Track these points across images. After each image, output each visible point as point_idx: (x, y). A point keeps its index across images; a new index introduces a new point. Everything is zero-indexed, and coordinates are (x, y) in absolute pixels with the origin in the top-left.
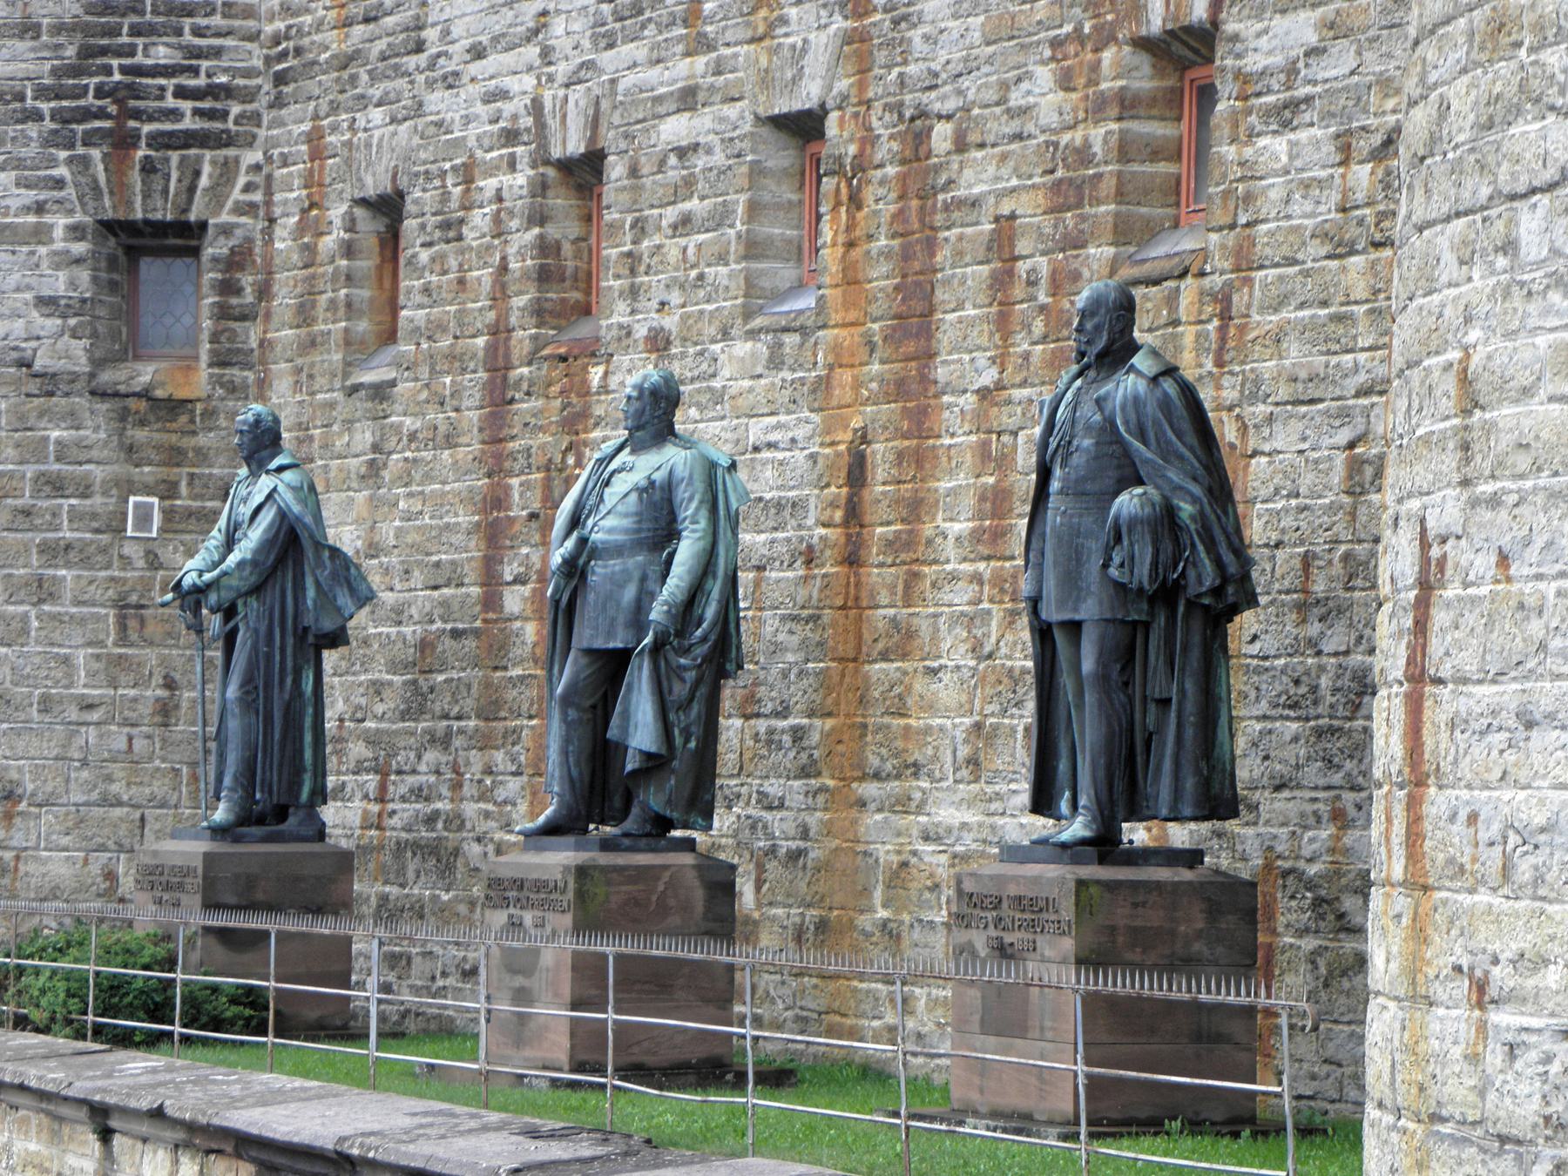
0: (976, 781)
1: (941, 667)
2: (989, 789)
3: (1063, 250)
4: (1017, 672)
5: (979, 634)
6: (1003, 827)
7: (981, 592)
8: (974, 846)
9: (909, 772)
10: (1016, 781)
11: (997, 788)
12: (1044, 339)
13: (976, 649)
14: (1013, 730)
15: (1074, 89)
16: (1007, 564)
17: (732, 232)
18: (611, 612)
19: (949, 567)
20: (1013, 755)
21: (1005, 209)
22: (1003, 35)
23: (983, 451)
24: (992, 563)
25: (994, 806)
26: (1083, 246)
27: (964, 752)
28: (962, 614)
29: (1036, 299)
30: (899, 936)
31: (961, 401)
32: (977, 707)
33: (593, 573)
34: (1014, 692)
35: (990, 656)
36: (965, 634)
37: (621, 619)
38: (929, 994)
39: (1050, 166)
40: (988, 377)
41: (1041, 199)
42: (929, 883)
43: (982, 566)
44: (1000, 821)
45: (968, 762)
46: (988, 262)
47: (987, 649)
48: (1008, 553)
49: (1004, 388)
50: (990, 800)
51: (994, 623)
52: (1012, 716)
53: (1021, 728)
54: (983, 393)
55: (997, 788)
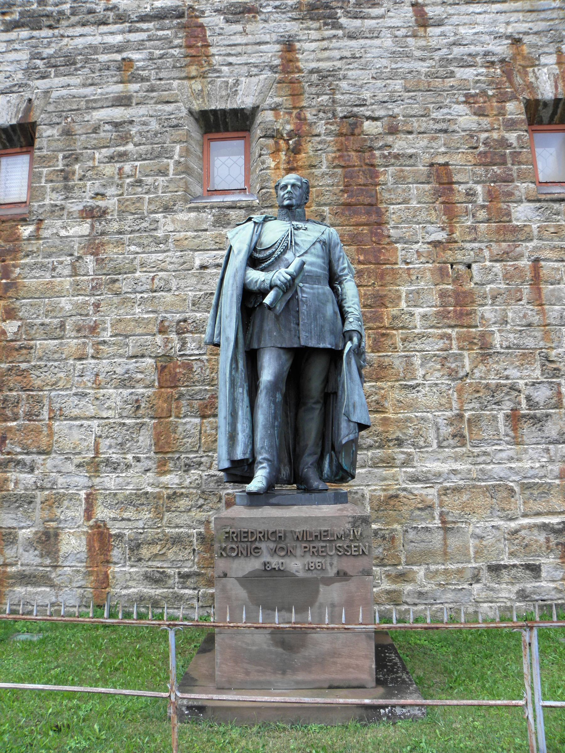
0: (463, 445)
1: (418, 385)
2: (476, 450)
3: (494, 182)
4: (493, 387)
5: (453, 366)
6: (491, 470)
7: (451, 344)
8: (461, 482)
9: (391, 444)
10: (499, 444)
11: (483, 449)
12: (488, 221)
13: (452, 375)
14: (495, 418)
15: (487, 116)
16: (474, 330)
17: (171, 162)
18: (320, 322)
19: (416, 331)
20: (497, 430)
21: (441, 160)
22: (423, 89)
23: (442, 273)
24: (456, 330)
25: (480, 459)
26: (512, 181)
27: (446, 431)
28: (435, 355)
29: (475, 201)
30: (393, 539)
31: (416, 246)
32: (455, 405)
33: (303, 291)
34: (493, 396)
35: (461, 379)
36: (439, 367)
37: (327, 327)
38: (428, 569)
39: (475, 145)
40: (441, 236)
41: (470, 158)
42: (420, 506)
43: (449, 331)
44: (489, 467)
45: (454, 436)
46: (428, 183)
47: (462, 374)
48: (473, 323)
49: (456, 242)
50: (478, 456)
51: (467, 361)
52: (492, 410)
53: (501, 416)
54: (436, 244)
55: (483, 449)
